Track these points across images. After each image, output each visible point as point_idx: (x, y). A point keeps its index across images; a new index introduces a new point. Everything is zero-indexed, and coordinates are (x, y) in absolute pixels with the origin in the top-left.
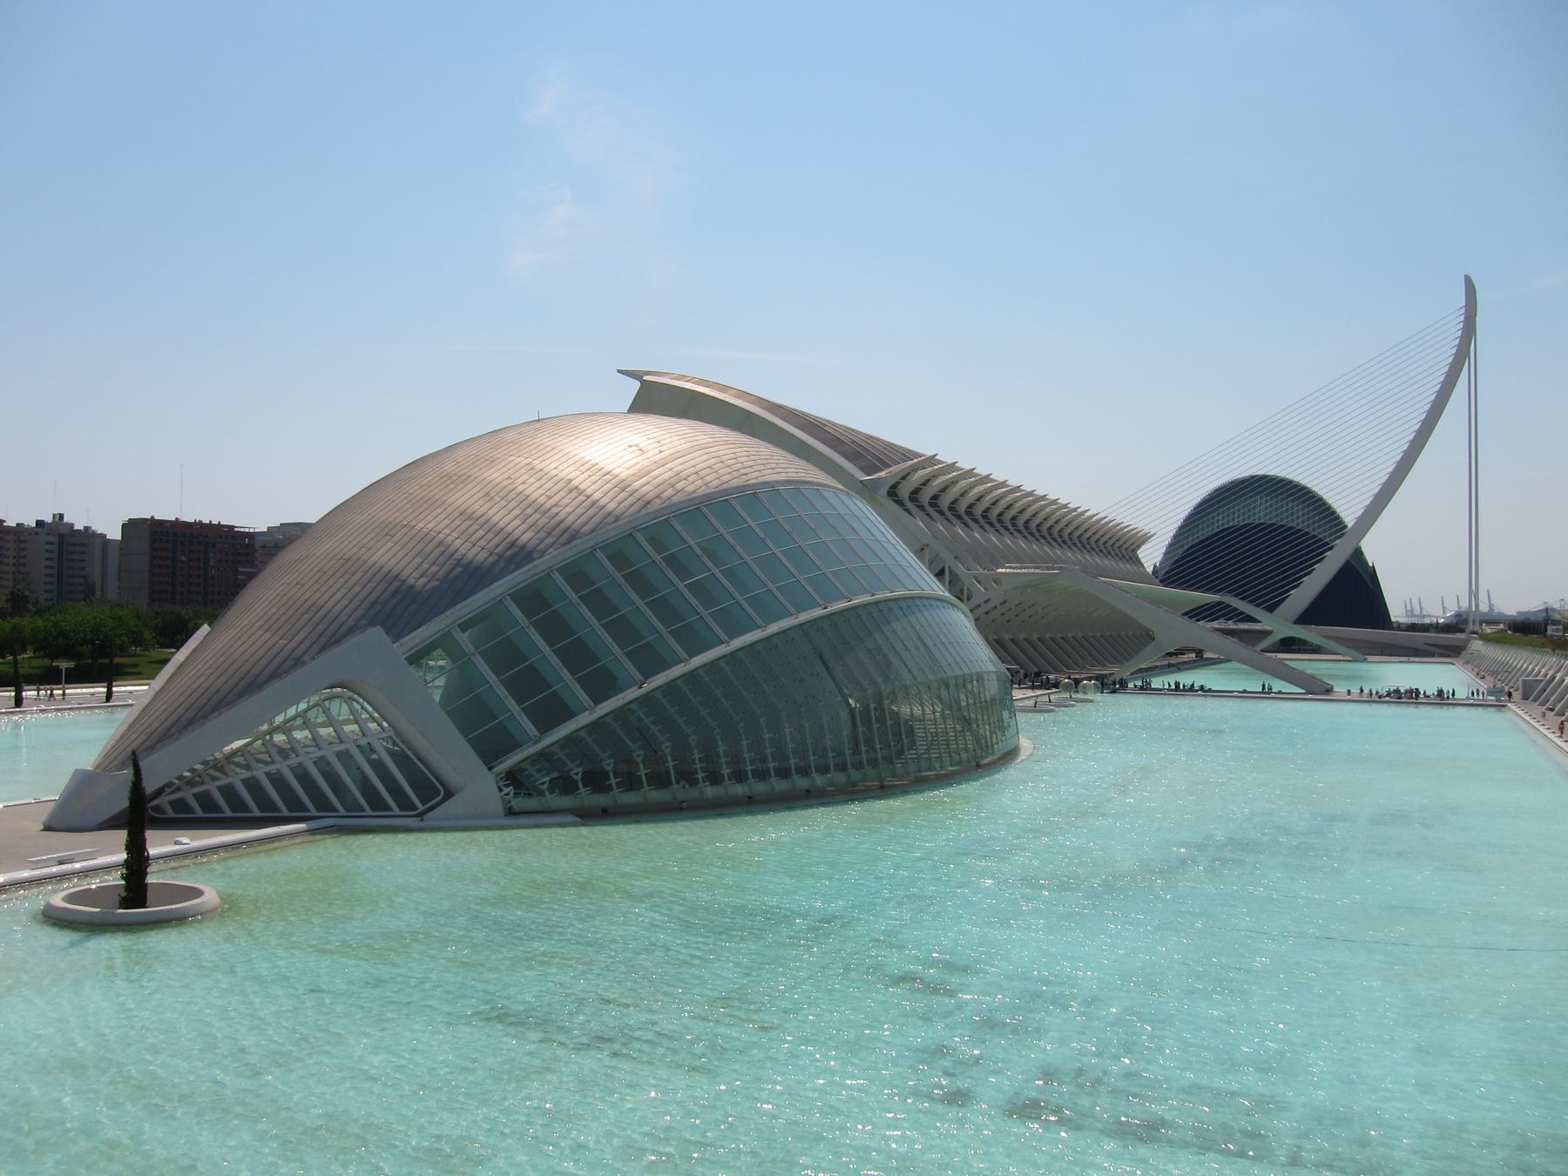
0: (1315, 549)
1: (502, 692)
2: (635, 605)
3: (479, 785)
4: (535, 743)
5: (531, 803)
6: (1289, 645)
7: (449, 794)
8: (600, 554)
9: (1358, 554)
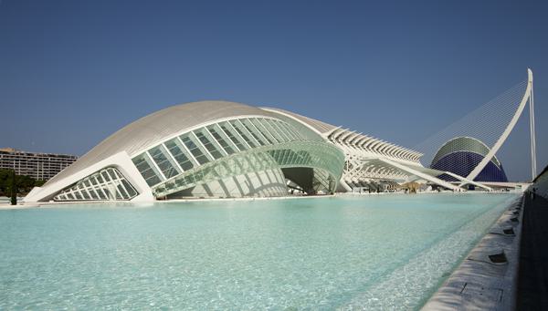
0: (480, 158)
6: (472, 187)
7: (138, 194)
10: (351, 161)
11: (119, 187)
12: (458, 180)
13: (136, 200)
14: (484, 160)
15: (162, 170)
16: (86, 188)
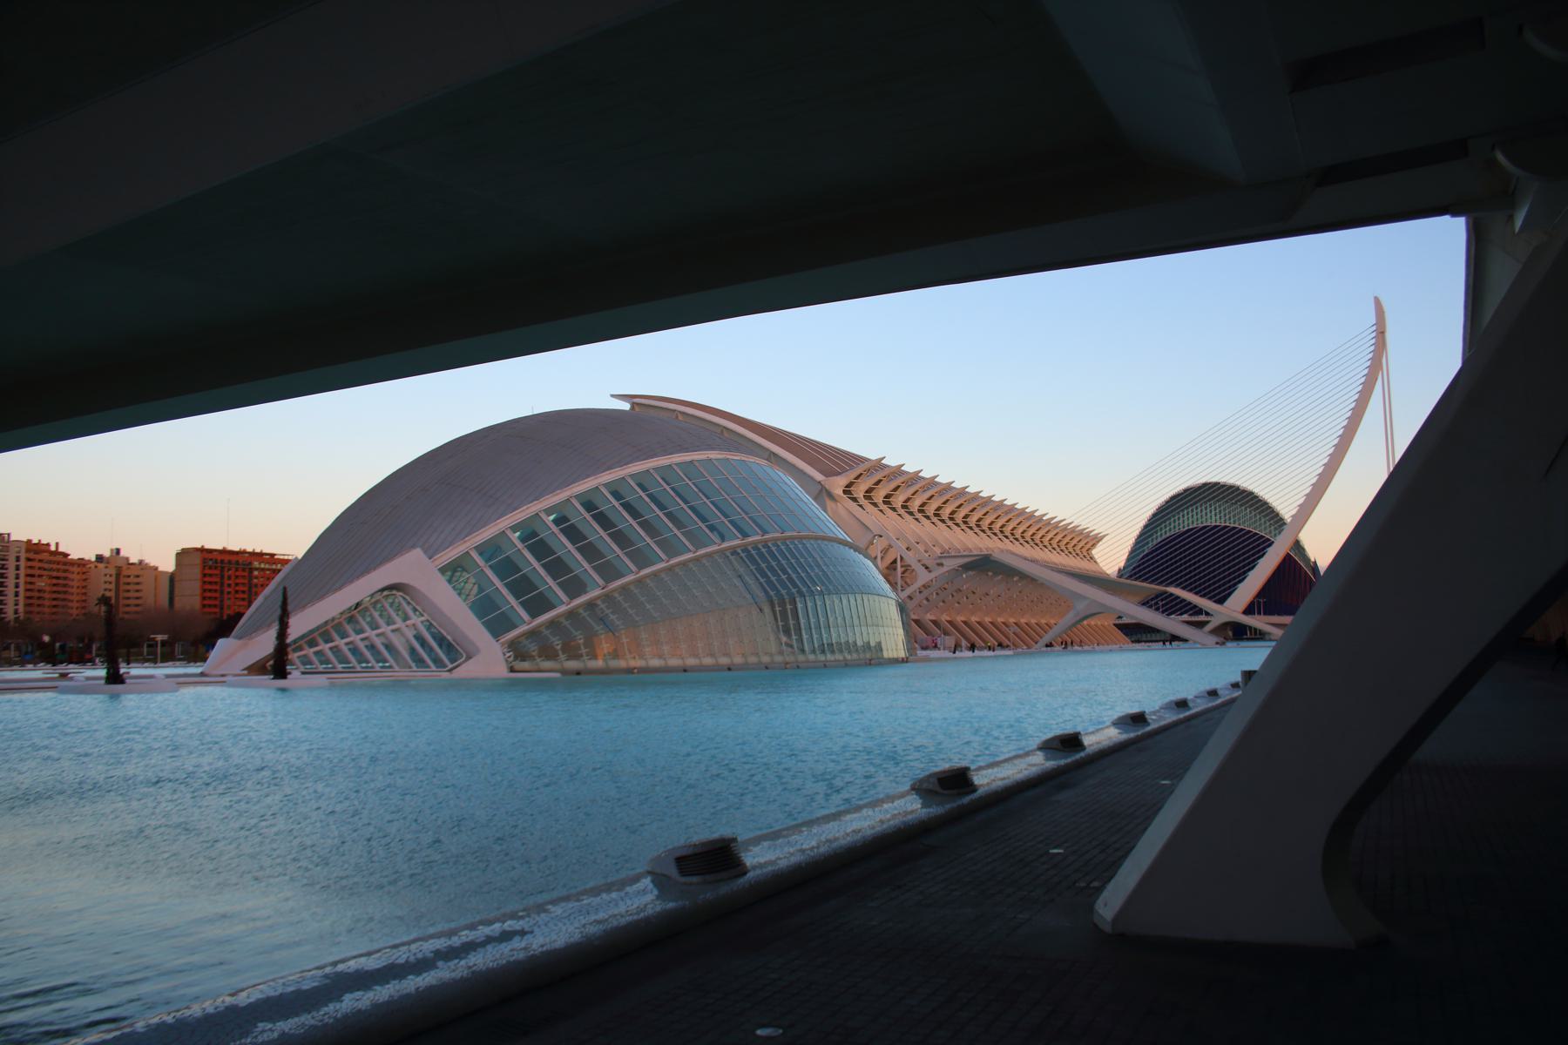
0: (1261, 545)
1: (505, 591)
2: (596, 534)
3: (489, 657)
4: (527, 623)
5: (526, 665)
7: (469, 658)
8: (575, 502)
9: (1298, 545)
10: (910, 558)
11: (419, 638)
12: (1200, 611)
13: (467, 670)
14: (1270, 550)
15: (517, 598)
16: (340, 642)
